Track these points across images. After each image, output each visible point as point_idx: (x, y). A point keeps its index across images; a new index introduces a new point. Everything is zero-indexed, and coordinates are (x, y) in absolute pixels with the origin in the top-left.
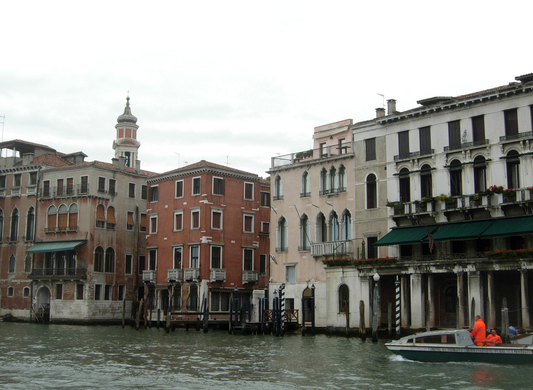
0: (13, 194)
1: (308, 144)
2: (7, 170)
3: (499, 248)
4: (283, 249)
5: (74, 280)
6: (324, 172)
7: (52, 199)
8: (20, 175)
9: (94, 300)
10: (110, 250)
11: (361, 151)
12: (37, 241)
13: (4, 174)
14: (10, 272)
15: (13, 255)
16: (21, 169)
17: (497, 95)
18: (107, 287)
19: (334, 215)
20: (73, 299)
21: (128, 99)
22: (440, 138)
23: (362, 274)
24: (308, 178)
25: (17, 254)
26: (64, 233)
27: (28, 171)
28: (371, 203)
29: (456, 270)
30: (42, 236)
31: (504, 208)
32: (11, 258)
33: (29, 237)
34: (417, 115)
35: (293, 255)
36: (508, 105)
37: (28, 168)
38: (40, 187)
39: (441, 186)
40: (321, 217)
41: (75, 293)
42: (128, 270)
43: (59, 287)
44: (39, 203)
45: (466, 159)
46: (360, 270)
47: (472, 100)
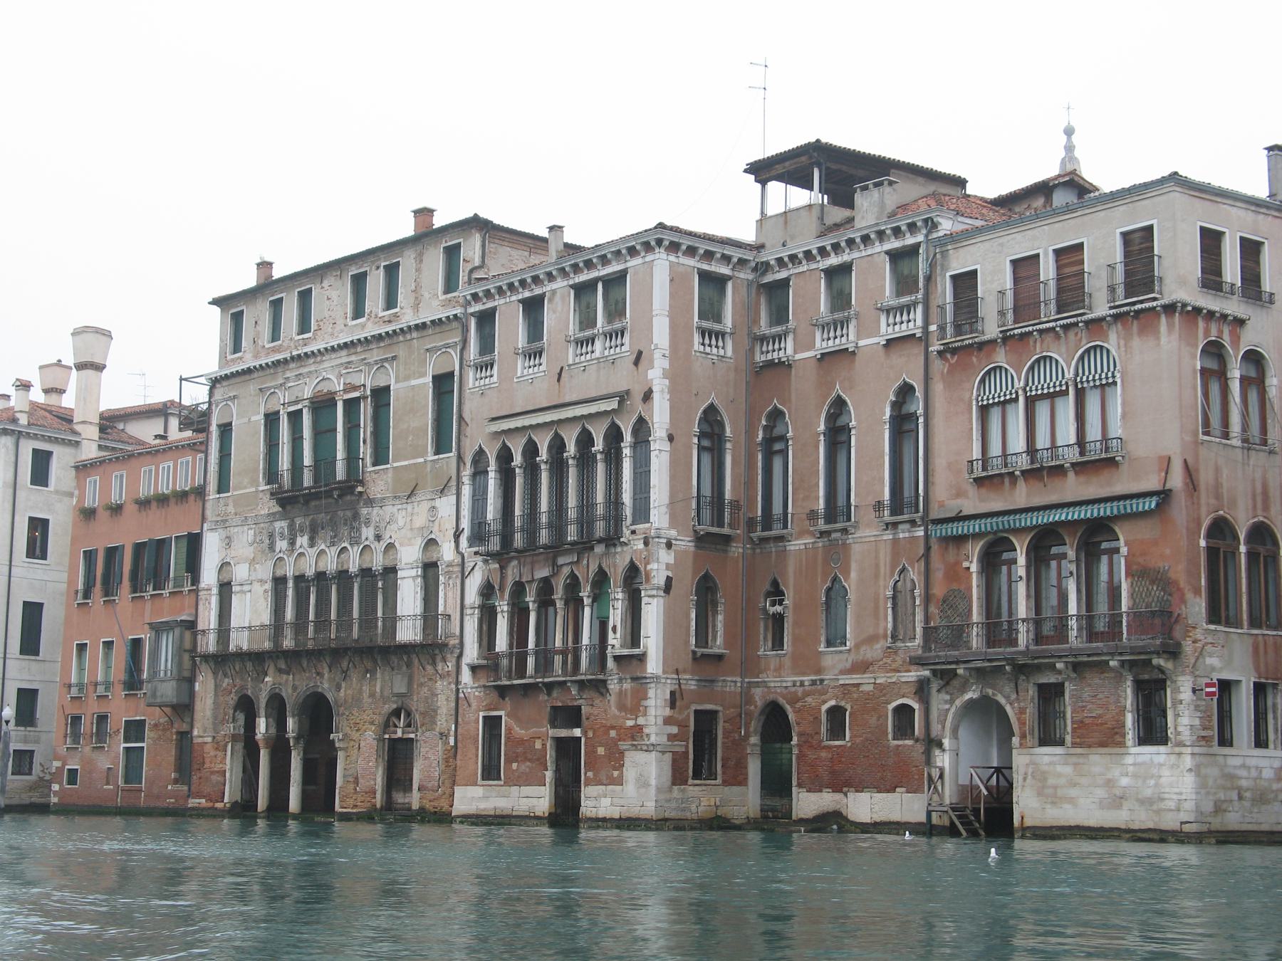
0: (822, 344)
2: (793, 258)
5: (1123, 663)
7: (992, 342)
8: (846, 269)
9: (1217, 749)
10: (1261, 533)
12: (934, 514)
13: (783, 275)
14: (829, 644)
15: (835, 579)
16: (851, 242)
20: (1122, 744)
25: (853, 575)
26: (1058, 471)
27: (878, 248)
30: (959, 494)
32: (829, 590)
33: (897, 504)
37: (881, 234)
38: (935, 301)
41: (1129, 719)
43: (1050, 695)
44: (938, 366)
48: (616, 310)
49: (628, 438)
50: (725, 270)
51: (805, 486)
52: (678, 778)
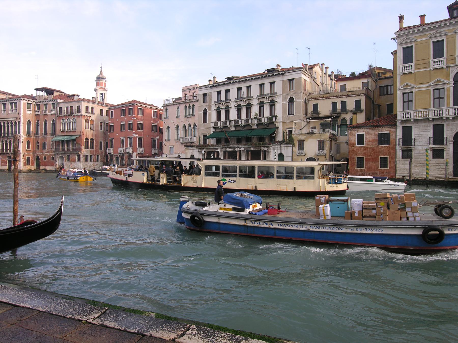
0: (44, 113)
1: (180, 94)
3: (255, 141)
4: (168, 140)
6: (186, 107)
8: (47, 104)
11: (201, 98)
17: (257, 77)
18: (91, 156)
19: (190, 126)
21: (101, 68)
22: (233, 94)
23: (200, 151)
24: (179, 109)
28: (205, 121)
29: (236, 150)
31: (257, 125)
34: (224, 84)
35: (173, 143)
36: (261, 82)
39: (233, 115)
40: (185, 126)
42: (101, 148)
43: (68, 156)
45: (243, 104)
46: (199, 149)
47: (247, 79)
48: (16, 107)
49: (17, 123)
50: (31, 102)
51: (41, 130)
52: (24, 165)
